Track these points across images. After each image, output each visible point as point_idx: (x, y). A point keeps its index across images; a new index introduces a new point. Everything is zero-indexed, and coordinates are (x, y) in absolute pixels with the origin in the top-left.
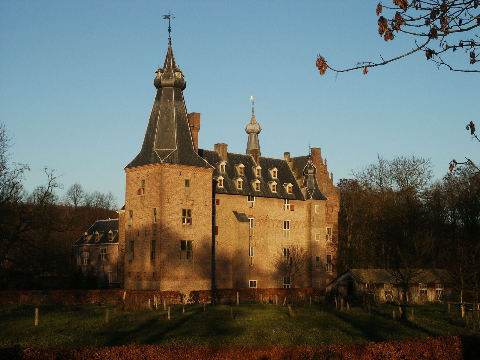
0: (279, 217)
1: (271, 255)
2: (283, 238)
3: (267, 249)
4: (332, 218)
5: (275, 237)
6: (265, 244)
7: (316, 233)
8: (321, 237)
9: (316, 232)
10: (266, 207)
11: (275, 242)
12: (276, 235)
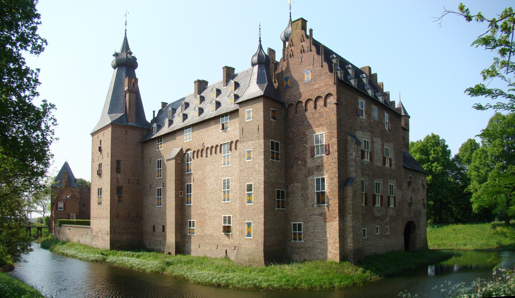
0: (216, 141)
1: (209, 190)
2: (223, 166)
3: (205, 183)
4: (325, 116)
5: (213, 167)
6: (203, 178)
7: (246, 150)
8: (255, 154)
9: (246, 149)
10: (202, 134)
11: (214, 174)
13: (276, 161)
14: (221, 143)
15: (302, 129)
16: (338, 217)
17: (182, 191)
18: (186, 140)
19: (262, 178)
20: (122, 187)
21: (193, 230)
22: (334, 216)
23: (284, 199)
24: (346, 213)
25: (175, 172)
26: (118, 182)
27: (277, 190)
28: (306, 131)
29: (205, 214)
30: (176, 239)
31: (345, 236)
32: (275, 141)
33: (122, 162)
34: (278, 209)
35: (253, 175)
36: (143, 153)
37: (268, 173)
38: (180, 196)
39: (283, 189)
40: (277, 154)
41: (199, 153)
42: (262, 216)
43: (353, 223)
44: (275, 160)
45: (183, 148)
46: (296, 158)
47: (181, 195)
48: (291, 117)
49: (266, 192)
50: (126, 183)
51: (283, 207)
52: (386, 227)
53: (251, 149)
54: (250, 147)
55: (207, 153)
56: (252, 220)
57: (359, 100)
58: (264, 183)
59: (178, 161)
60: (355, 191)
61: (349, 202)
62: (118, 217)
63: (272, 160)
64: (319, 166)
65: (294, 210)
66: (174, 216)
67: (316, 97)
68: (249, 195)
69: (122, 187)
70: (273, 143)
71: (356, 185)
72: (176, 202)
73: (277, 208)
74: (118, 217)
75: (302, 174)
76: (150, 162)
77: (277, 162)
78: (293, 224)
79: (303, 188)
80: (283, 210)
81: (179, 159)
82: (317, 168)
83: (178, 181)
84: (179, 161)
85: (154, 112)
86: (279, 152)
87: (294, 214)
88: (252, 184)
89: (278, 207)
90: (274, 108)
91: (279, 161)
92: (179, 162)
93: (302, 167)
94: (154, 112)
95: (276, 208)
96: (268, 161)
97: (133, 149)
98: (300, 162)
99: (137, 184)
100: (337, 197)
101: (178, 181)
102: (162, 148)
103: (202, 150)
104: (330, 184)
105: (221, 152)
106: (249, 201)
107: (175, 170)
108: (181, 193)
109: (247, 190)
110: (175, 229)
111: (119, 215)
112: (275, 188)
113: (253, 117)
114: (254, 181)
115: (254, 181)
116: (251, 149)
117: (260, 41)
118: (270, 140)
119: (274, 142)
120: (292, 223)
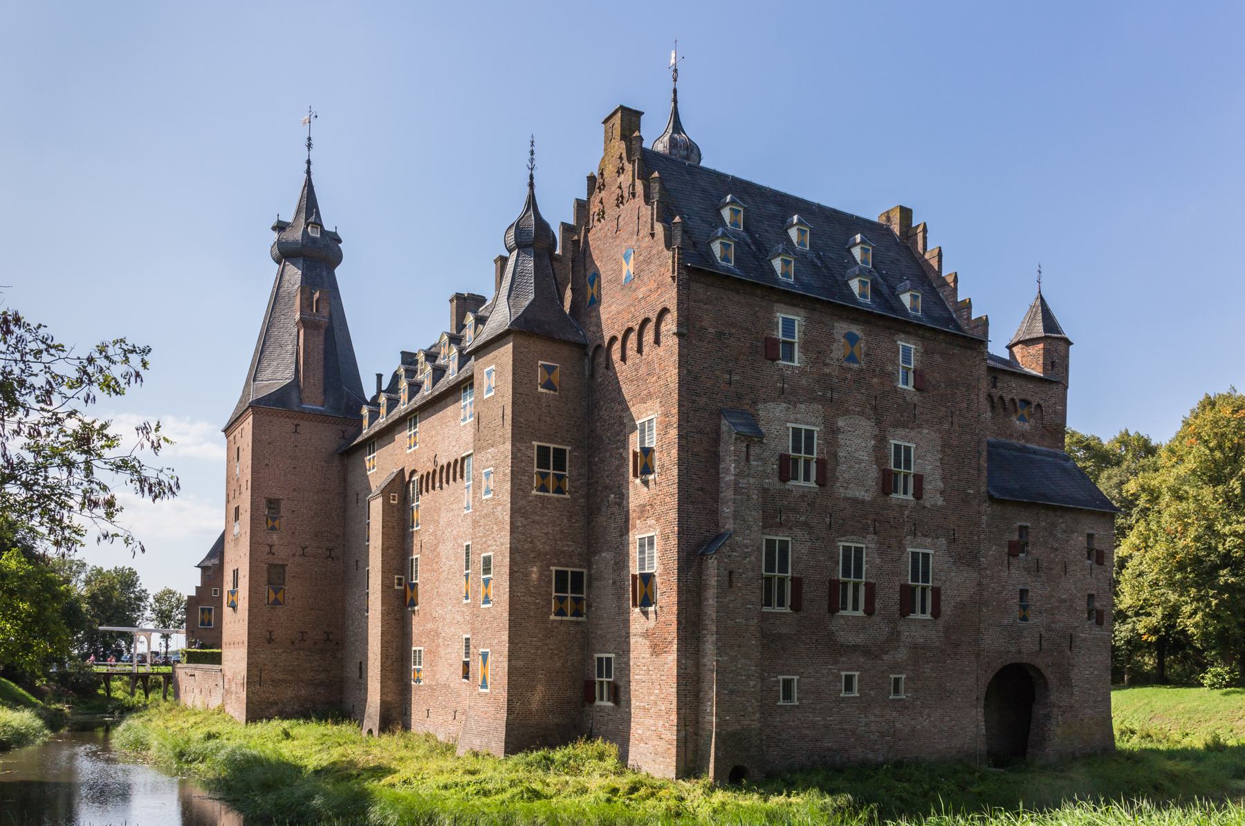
6: (435, 542)
12: (454, 507)
13: (556, 495)
14: (463, 455)
15: (617, 411)
16: (676, 641)
17: (403, 574)
18: (410, 448)
19: (505, 538)
20: (283, 566)
21: (419, 671)
22: (670, 639)
23: (583, 594)
24: (704, 632)
25: (383, 527)
26: (273, 554)
27: (556, 571)
28: (624, 415)
29: (437, 634)
30: (382, 694)
31: (701, 694)
32: (552, 446)
33: (283, 504)
34: (559, 618)
35: (492, 533)
36: (344, 480)
37: (524, 526)
38: (396, 587)
39: (581, 566)
40: (560, 478)
41: (430, 481)
42: (505, 636)
43: (717, 661)
44: (551, 494)
45: (405, 469)
46: (606, 487)
47: (400, 584)
48: (600, 380)
49: (516, 575)
50: (294, 555)
51: (577, 613)
52: (892, 676)
53: (491, 469)
54: (488, 463)
55: (441, 481)
56: (491, 645)
57: (778, 314)
58: (511, 553)
59: (392, 502)
60: (731, 573)
61: (711, 602)
62: (270, 641)
63: (542, 494)
64: (644, 506)
65: (601, 622)
66: (380, 638)
67: (640, 322)
68: (487, 582)
69: (283, 566)
70: (543, 452)
71: (735, 554)
72: (383, 604)
73: (555, 615)
74: (270, 641)
75: (615, 528)
76: (357, 502)
77: (558, 500)
78: (598, 658)
79: (616, 564)
80: (578, 623)
81: (394, 496)
82: (642, 512)
83: (390, 551)
84: (394, 500)
85: (379, 377)
86: (567, 473)
87: (600, 632)
88: (490, 556)
89: (561, 612)
90: (552, 360)
91: (567, 496)
92: (396, 502)
93: (615, 509)
94: (379, 377)
95: (552, 617)
96: (525, 497)
97: (317, 470)
98: (613, 496)
99: (327, 558)
100: (675, 588)
101: (390, 551)
102: (375, 470)
103: (435, 471)
104: (664, 552)
105: (462, 477)
106: (487, 600)
107: (383, 522)
108: (400, 579)
109: (484, 570)
110: (382, 670)
111: (273, 637)
112: (548, 566)
113: (496, 386)
114: (494, 547)
115: (494, 547)
116: (491, 469)
117: (531, 185)
118: (535, 443)
119: (549, 448)
120: (597, 655)
